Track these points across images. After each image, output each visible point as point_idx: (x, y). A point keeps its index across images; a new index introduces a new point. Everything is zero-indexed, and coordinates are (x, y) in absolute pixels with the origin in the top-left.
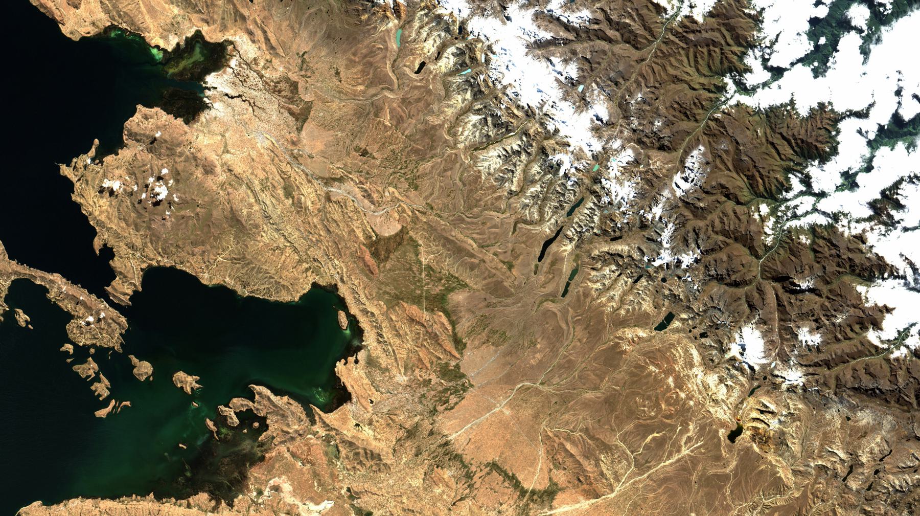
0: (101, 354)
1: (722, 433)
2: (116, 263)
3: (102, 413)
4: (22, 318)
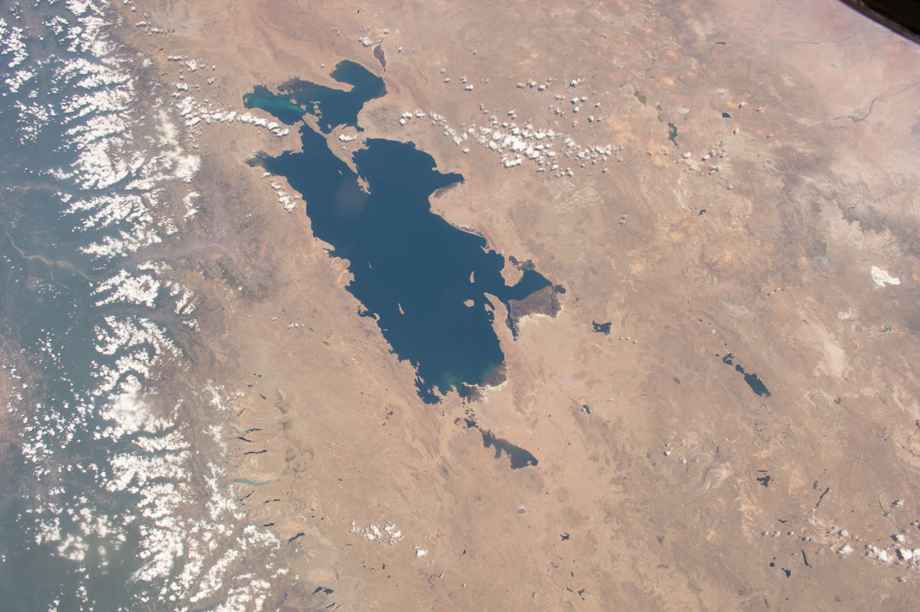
0: (313, 112)
1: (164, 50)
2: (300, 129)
3: (319, 102)
4: (330, 126)
